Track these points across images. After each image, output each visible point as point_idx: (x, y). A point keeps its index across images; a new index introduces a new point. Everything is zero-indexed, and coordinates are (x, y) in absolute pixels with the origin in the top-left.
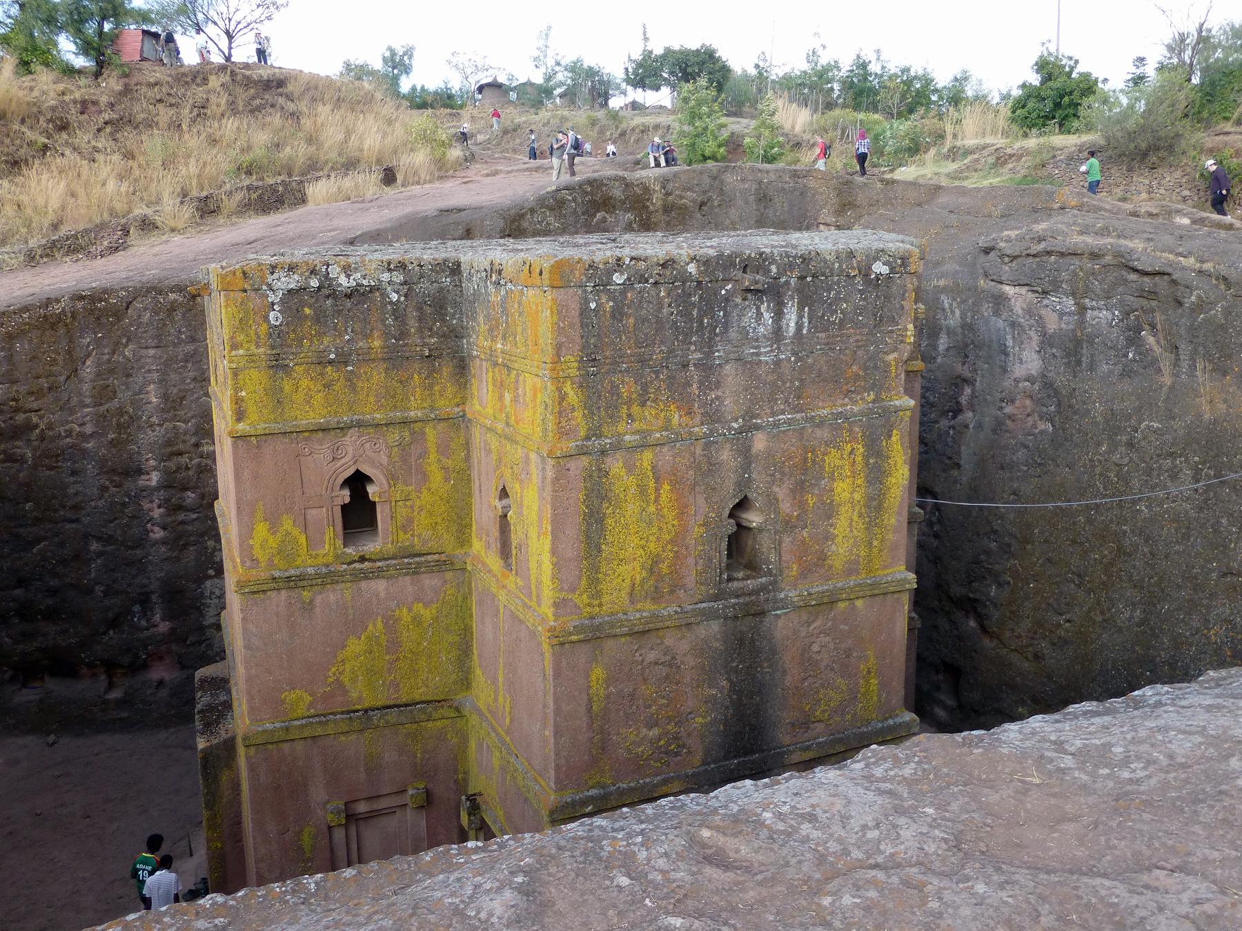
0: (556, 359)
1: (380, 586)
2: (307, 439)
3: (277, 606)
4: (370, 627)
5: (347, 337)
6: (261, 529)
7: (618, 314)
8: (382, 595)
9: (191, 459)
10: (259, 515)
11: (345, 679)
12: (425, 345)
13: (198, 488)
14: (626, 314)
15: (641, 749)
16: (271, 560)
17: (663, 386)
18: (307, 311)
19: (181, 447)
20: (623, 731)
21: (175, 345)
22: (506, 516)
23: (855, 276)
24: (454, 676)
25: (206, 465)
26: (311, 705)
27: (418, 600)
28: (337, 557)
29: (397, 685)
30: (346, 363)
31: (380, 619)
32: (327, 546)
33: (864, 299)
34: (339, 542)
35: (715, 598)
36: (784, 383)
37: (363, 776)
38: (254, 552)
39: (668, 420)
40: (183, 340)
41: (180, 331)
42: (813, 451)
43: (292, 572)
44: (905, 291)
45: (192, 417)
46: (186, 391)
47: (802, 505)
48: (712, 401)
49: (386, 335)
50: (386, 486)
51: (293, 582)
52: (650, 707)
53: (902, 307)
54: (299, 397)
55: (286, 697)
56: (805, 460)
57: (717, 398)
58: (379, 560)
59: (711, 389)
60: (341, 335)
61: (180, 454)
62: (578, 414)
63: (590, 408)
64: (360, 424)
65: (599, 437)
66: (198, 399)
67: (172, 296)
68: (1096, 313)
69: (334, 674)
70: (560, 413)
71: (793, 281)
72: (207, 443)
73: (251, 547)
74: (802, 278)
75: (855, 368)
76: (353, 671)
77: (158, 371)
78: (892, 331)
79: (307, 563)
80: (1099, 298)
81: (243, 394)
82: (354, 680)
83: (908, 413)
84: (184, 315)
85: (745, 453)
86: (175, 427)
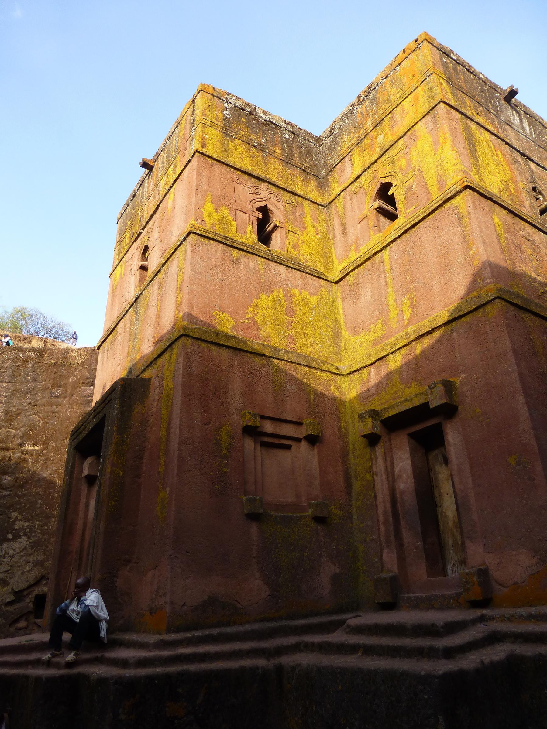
4: (275, 293)
9: (14, 453)
10: (209, 198)
11: (258, 319)
13: (14, 473)
19: (9, 445)
21: (22, 382)
24: (331, 349)
25: (25, 458)
29: (293, 339)
31: (281, 290)
37: (270, 397)
38: (204, 216)
40: (28, 380)
41: (28, 374)
45: (22, 426)
46: (22, 410)
55: (216, 314)
61: (7, 449)
66: (29, 415)
67: (28, 354)
69: (251, 313)
72: (28, 445)
76: (263, 316)
77: (6, 396)
81: (207, 136)
82: (265, 323)
84: (33, 365)
86: (8, 432)
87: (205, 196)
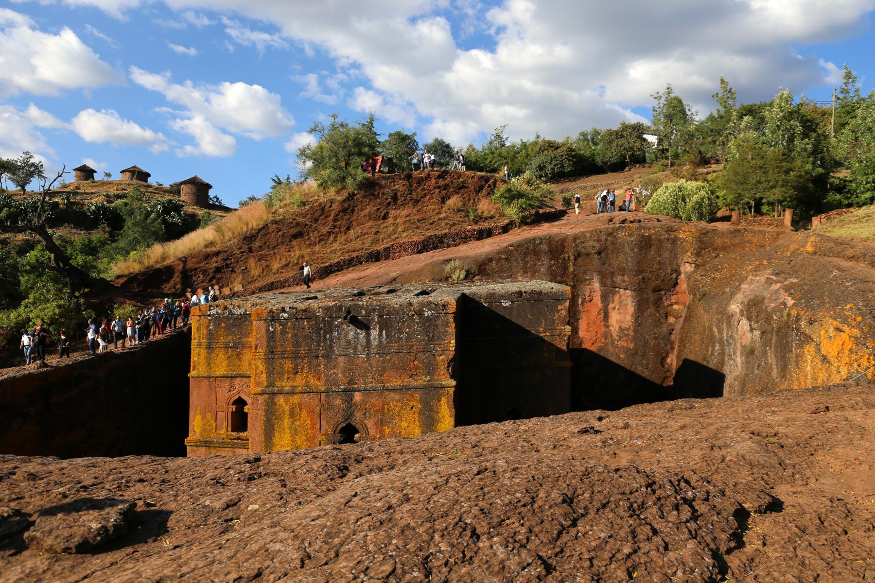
2: (221, 380)
7: (284, 332)
10: (198, 412)
14: (287, 332)
18: (223, 325)
23: (413, 315)
28: (227, 436)
30: (237, 348)
34: (230, 429)
36: (372, 368)
39: (307, 382)
42: (388, 404)
43: (208, 439)
54: (217, 361)
56: (383, 408)
59: (331, 369)
62: (264, 376)
63: (270, 373)
65: (273, 386)
71: (376, 318)
74: (380, 316)
75: (416, 363)
78: (440, 344)
79: (213, 437)
83: (452, 389)
85: (349, 401)
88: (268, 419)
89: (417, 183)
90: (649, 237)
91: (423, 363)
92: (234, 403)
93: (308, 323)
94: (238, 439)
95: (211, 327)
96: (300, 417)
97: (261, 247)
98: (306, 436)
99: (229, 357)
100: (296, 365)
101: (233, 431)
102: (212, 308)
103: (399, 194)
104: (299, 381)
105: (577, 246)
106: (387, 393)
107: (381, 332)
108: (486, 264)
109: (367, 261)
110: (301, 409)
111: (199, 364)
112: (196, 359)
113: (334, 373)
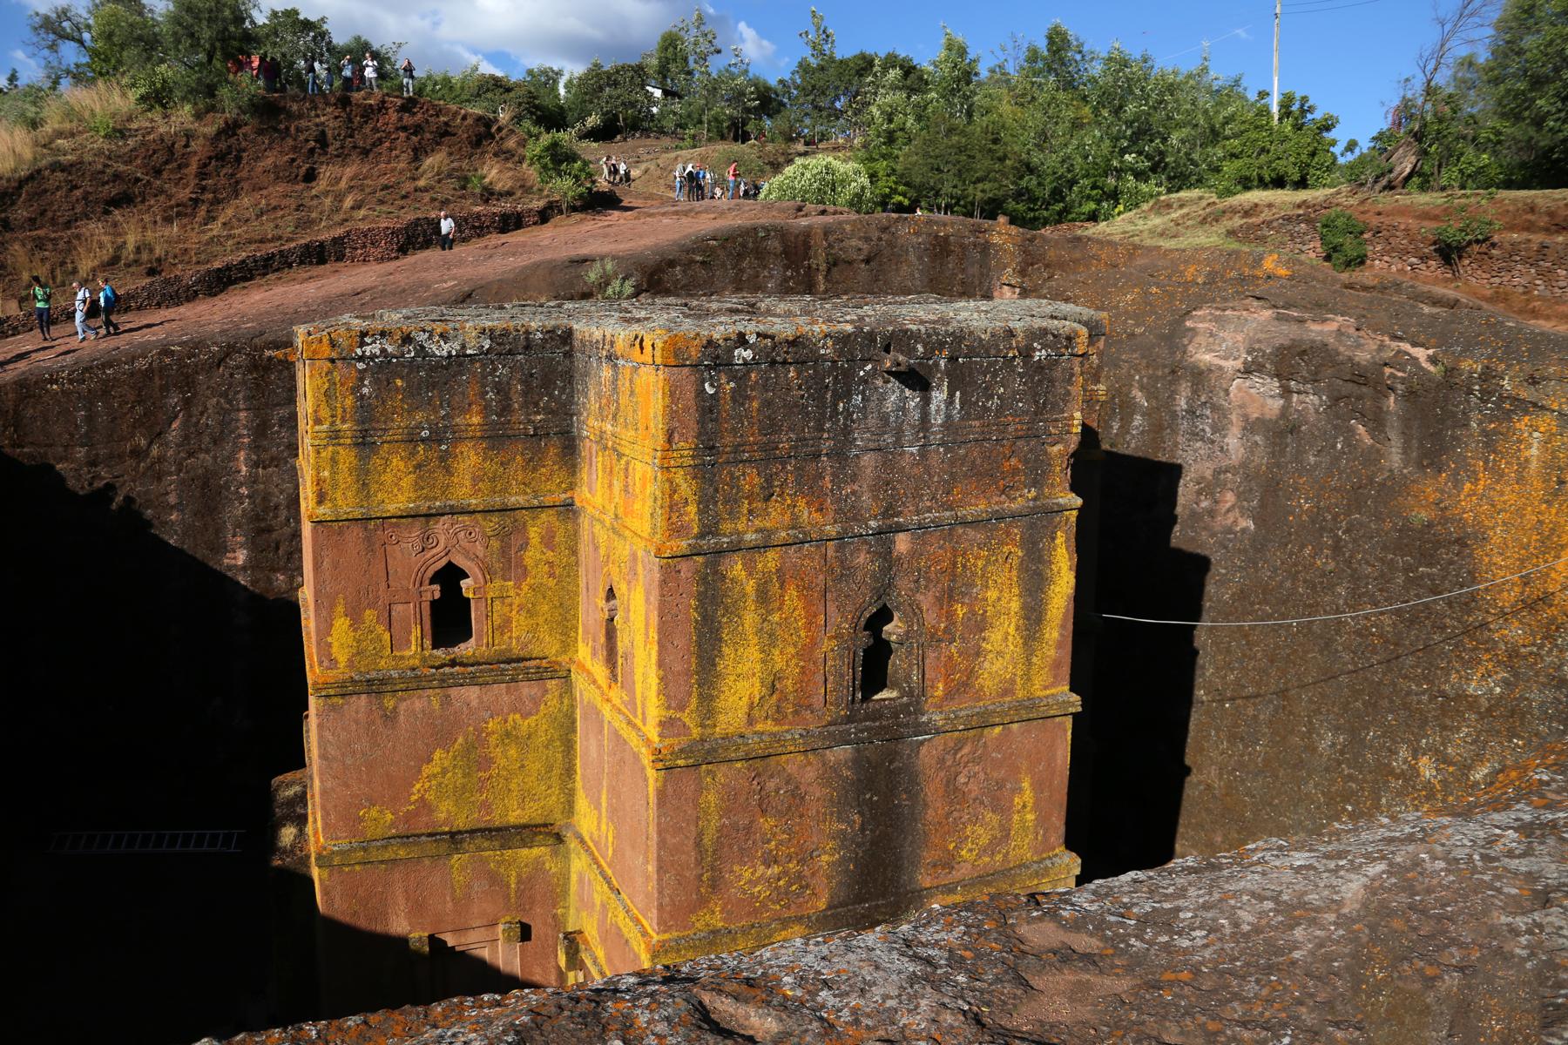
0: (667, 446)
1: (472, 693)
2: (397, 525)
3: (357, 713)
5: (443, 413)
6: (341, 624)
7: (739, 396)
8: (474, 703)
10: (340, 609)
12: (530, 421)
14: (748, 397)
15: (757, 889)
16: (350, 660)
17: (791, 478)
18: (399, 383)
20: (736, 868)
22: (612, 620)
26: (393, 824)
27: (515, 710)
28: (424, 659)
29: (489, 806)
30: (440, 442)
32: (413, 648)
33: (1025, 384)
34: (428, 643)
35: (849, 720)
36: (931, 476)
39: (795, 517)
43: (373, 675)
44: (1072, 375)
47: (950, 615)
48: (847, 496)
49: (486, 410)
50: (482, 581)
51: (375, 687)
52: (769, 842)
53: (1068, 393)
54: (388, 478)
56: (954, 564)
57: (854, 493)
58: (472, 665)
60: (436, 412)
62: (692, 509)
63: (705, 503)
64: (454, 512)
65: (715, 534)
68: (1302, 397)
70: (671, 507)
71: (942, 363)
73: (330, 645)
74: (952, 359)
75: (1013, 461)
78: (1056, 420)
80: (1305, 382)
83: (1075, 513)
85: (886, 555)
87: (332, 607)
88: (705, 618)
89: (362, 117)
90: (946, 238)
91: (1026, 462)
92: (437, 578)
93: (799, 374)
94: (453, 663)
95: (365, 390)
96: (782, 604)
97: (32, 221)
98: (795, 646)
99: (419, 466)
100: (769, 480)
101: (435, 646)
102: (367, 340)
103: (329, 134)
104: (776, 517)
105: (830, 246)
106: (960, 531)
107: (951, 395)
108: (663, 271)
109: (301, 263)
110: (782, 587)
111: (335, 486)
112: (326, 474)
113: (854, 493)
